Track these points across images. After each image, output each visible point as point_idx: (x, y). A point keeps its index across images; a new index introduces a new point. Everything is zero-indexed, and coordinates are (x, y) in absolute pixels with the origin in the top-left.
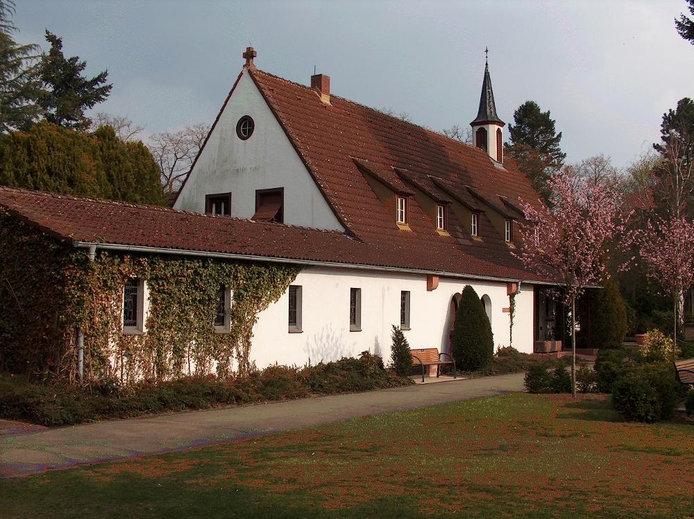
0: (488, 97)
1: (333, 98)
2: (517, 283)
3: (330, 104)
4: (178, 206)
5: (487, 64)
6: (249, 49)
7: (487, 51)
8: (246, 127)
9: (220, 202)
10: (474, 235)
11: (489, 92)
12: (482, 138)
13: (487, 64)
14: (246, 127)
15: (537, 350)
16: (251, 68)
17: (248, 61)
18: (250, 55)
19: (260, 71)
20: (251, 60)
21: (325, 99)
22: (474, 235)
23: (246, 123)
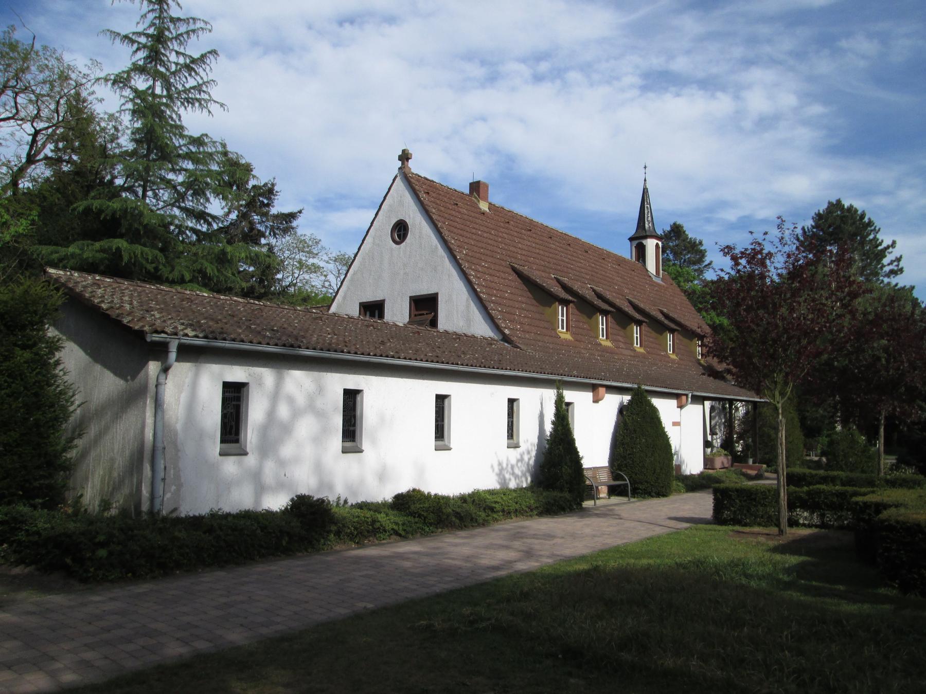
0: (646, 212)
1: (491, 206)
2: (687, 395)
3: (488, 211)
4: (333, 309)
5: (645, 180)
6: (404, 151)
7: (645, 167)
8: (400, 230)
9: (374, 309)
10: (636, 346)
11: (647, 207)
12: (641, 252)
13: (645, 180)
14: (400, 230)
15: (706, 465)
16: (406, 170)
17: (403, 164)
18: (405, 157)
19: (416, 174)
20: (406, 163)
21: (484, 206)
22: (636, 346)
23: (400, 228)
